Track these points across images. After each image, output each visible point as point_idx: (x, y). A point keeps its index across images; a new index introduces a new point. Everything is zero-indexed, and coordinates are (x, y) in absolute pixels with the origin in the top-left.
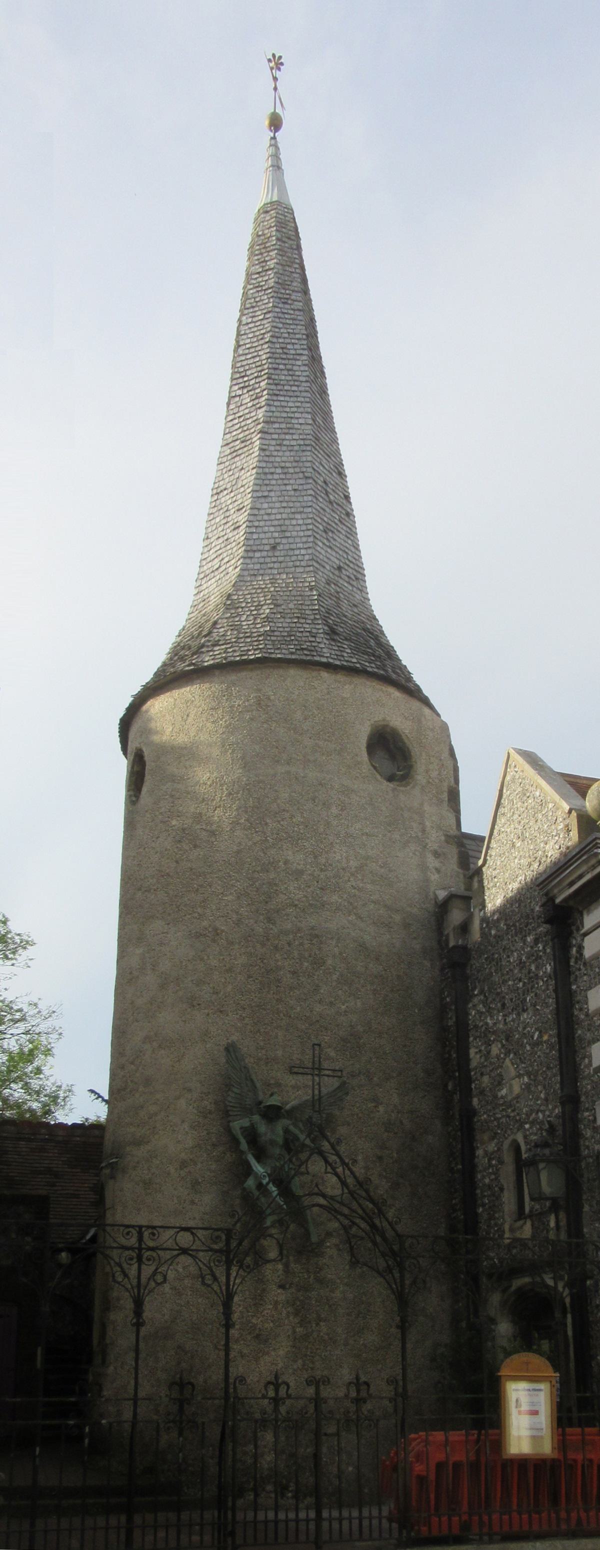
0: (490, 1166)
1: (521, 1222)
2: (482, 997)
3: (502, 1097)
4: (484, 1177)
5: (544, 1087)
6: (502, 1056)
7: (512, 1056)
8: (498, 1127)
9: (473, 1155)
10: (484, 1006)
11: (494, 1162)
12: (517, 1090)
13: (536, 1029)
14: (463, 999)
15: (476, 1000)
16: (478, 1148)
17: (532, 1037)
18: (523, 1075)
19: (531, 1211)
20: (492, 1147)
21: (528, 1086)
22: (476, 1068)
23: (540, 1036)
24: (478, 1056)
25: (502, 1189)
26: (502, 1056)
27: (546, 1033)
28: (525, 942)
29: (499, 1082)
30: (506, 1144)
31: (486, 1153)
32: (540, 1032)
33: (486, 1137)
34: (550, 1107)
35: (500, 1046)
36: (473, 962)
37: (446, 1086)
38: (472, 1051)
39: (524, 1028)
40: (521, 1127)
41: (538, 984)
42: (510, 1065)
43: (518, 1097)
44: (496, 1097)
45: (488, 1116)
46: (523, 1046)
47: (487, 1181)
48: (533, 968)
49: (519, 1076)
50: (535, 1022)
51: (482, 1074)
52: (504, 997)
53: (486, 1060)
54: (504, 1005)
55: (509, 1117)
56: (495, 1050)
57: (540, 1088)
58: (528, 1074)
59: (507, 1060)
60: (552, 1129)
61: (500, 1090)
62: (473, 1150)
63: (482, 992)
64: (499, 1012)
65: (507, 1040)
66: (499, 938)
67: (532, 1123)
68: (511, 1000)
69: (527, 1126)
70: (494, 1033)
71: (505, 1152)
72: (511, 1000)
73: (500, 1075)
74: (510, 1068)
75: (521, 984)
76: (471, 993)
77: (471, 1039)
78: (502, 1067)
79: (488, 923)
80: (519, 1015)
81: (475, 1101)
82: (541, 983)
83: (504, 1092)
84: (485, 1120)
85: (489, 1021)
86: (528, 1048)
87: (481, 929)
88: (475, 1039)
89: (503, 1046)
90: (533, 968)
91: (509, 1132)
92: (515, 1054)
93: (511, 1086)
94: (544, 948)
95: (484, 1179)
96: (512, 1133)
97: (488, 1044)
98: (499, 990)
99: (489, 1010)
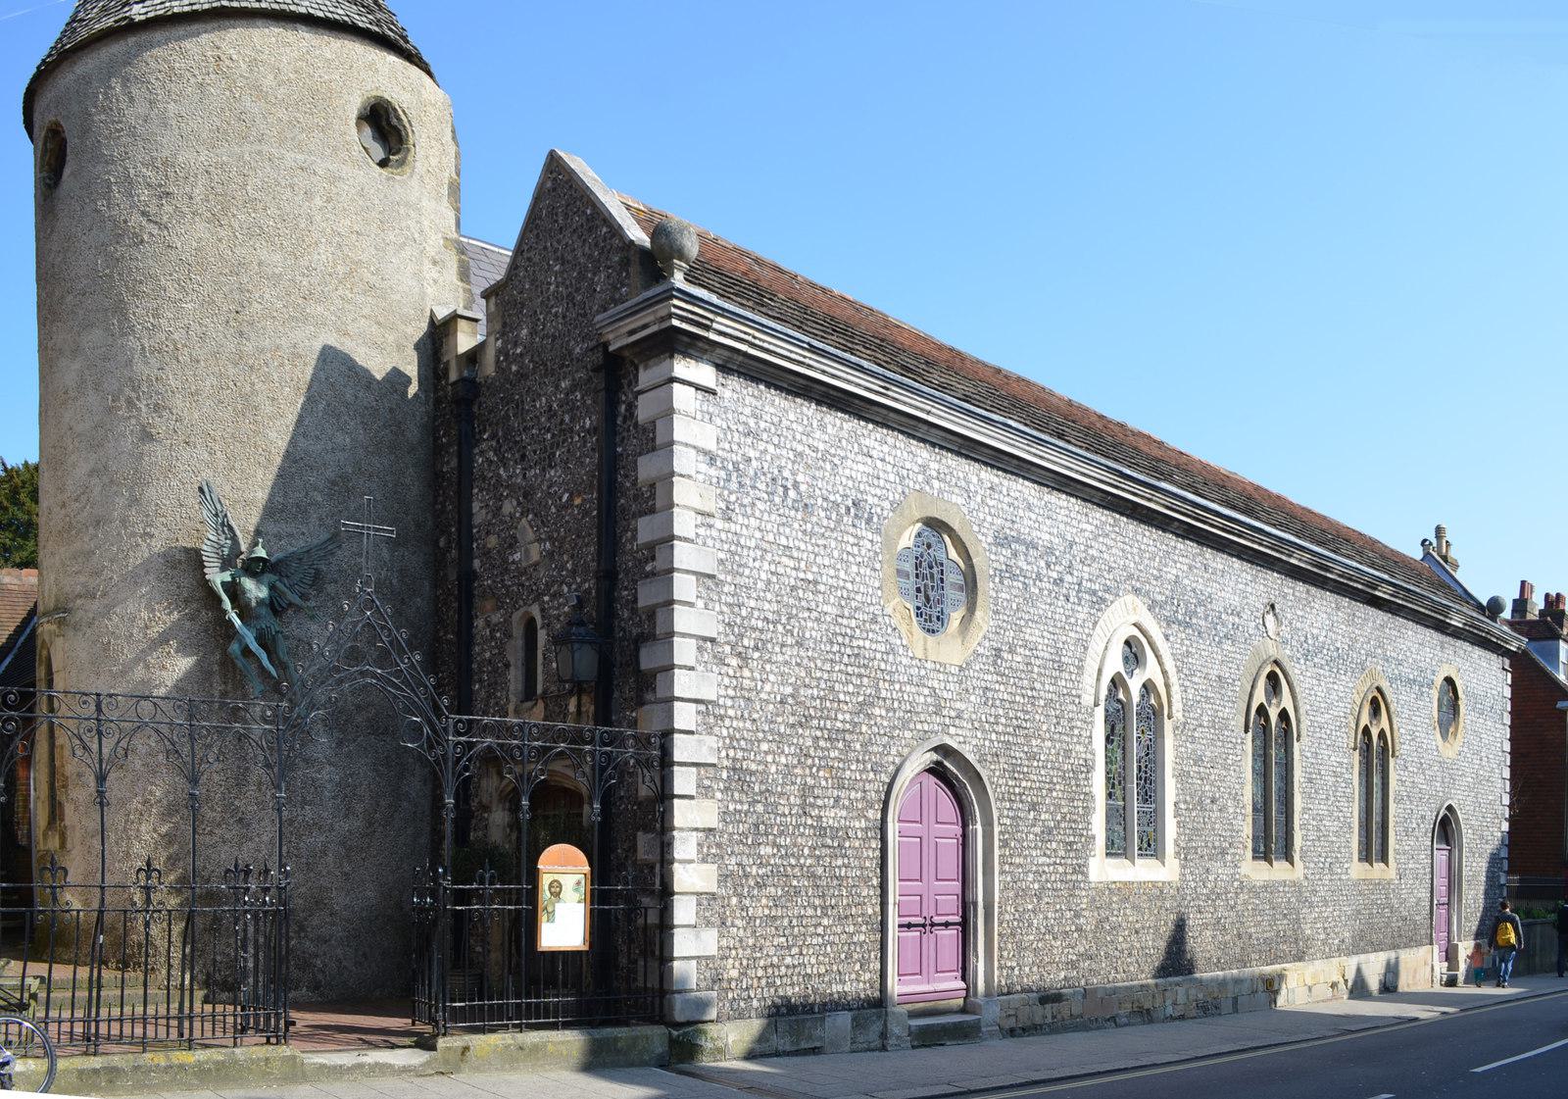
0: (493, 637)
1: (529, 704)
2: (494, 443)
3: (513, 562)
4: (484, 651)
5: (572, 557)
6: (518, 515)
7: (530, 516)
8: (507, 595)
9: (471, 625)
10: (496, 454)
11: (498, 635)
12: (535, 557)
13: (566, 491)
14: (467, 443)
15: (484, 446)
16: (477, 617)
17: (560, 498)
18: (544, 541)
19: (545, 692)
20: (497, 618)
21: (551, 554)
22: (480, 526)
23: (571, 498)
24: (484, 511)
25: (507, 666)
26: (518, 515)
27: (579, 495)
28: (557, 387)
29: (512, 544)
30: (517, 616)
31: (488, 624)
32: (571, 495)
33: (489, 605)
34: (579, 580)
35: (515, 503)
36: (482, 399)
37: (437, 542)
38: (476, 506)
39: (549, 487)
40: (538, 598)
41: (572, 438)
42: (528, 527)
43: (536, 564)
44: (505, 561)
45: (494, 581)
46: (547, 507)
47: (488, 655)
48: (567, 418)
49: (539, 540)
50: (565, 481)
51: (488, 533)
52: (525, 447)
53: (494, 517)
54: (523, 457)
55: (523, 585)
56: (508, 507)
57: (565, 557)
58: (550, 538)
59: (524, 520)
60: (581, 603)
61: (512, 554)
62: (470, 619)
63: (493, 436)
64: (516, 462)
65: (525, 497)
66: (522, 376)
67: (554, 596)
68: (535, 452)
69: (546, 598)
70: (507, 487)
71: (514, 624)
72: (535, 452)
73: (514, 537)
74: (526, 530)
75: (549, 436)
76: (477, 437)
77: (476, 491)
78: (516, 528)
79: (507, 355)
80: (544, 470)
81: (477, 563)
82: (577, 438)
83: (517, 556)
84: (488, 586)
85: (501, 471)
86: (553, 510)
87: (497, 361)
88: (481, 490)
89: (519, 504)
90: (567, 418)
91: (521, 603)
92: (536, 515)
93: (527, 551)
94: (582, 398)
95: (483, 652)
96: (525, 604)
97: (500, 498)
98: (518, 439)
99: (503, 462)
